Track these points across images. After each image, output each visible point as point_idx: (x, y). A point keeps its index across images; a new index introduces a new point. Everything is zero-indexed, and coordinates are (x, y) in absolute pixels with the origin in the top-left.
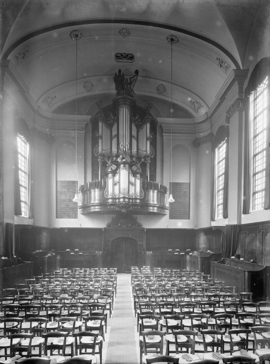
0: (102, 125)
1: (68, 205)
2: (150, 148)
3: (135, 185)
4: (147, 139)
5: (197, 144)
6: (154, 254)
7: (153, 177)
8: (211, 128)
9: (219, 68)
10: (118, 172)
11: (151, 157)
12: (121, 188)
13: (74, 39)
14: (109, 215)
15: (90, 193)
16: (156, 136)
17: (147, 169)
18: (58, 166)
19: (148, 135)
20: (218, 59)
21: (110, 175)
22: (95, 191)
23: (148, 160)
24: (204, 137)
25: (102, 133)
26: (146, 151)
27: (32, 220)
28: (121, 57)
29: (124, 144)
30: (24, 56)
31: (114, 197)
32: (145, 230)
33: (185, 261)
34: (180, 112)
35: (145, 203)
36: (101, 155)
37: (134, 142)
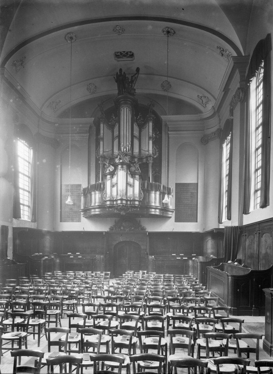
0: (104, 126)
1: (71, 209)
2: (153, 147)
3: (133, 186)
4: (149, 138)
5: (205, 140)
6: (156, 259)
7: (157, 178)
8: (220, 123)
9: (221, 57)
10: (115, 173)
11: (153, 157)
12: (118, 189)
13: (69, 42)
14: (112, 218)
15: (91, 195)
16: (162, 135)
17: (149, 168)
18: (63, 170)
19: (151, 134)
20: (218, 48)
21: (108, 177)
22: (95, 194)
23: (150, 160)
24: (212, 133)
25: (103, 134)
26: (148, 151)
27: (36, 224)
28: (121, 56)
29: (125, 145)
30: (22, 63)
31: (112, 199)
32: (147, 234)
33: (187, 266)
34: (180, 106)
35: (145, 205)
36: (102, 157)
37: (136, 142)
